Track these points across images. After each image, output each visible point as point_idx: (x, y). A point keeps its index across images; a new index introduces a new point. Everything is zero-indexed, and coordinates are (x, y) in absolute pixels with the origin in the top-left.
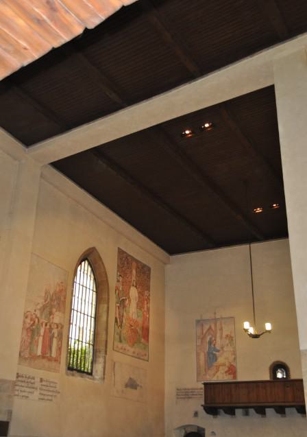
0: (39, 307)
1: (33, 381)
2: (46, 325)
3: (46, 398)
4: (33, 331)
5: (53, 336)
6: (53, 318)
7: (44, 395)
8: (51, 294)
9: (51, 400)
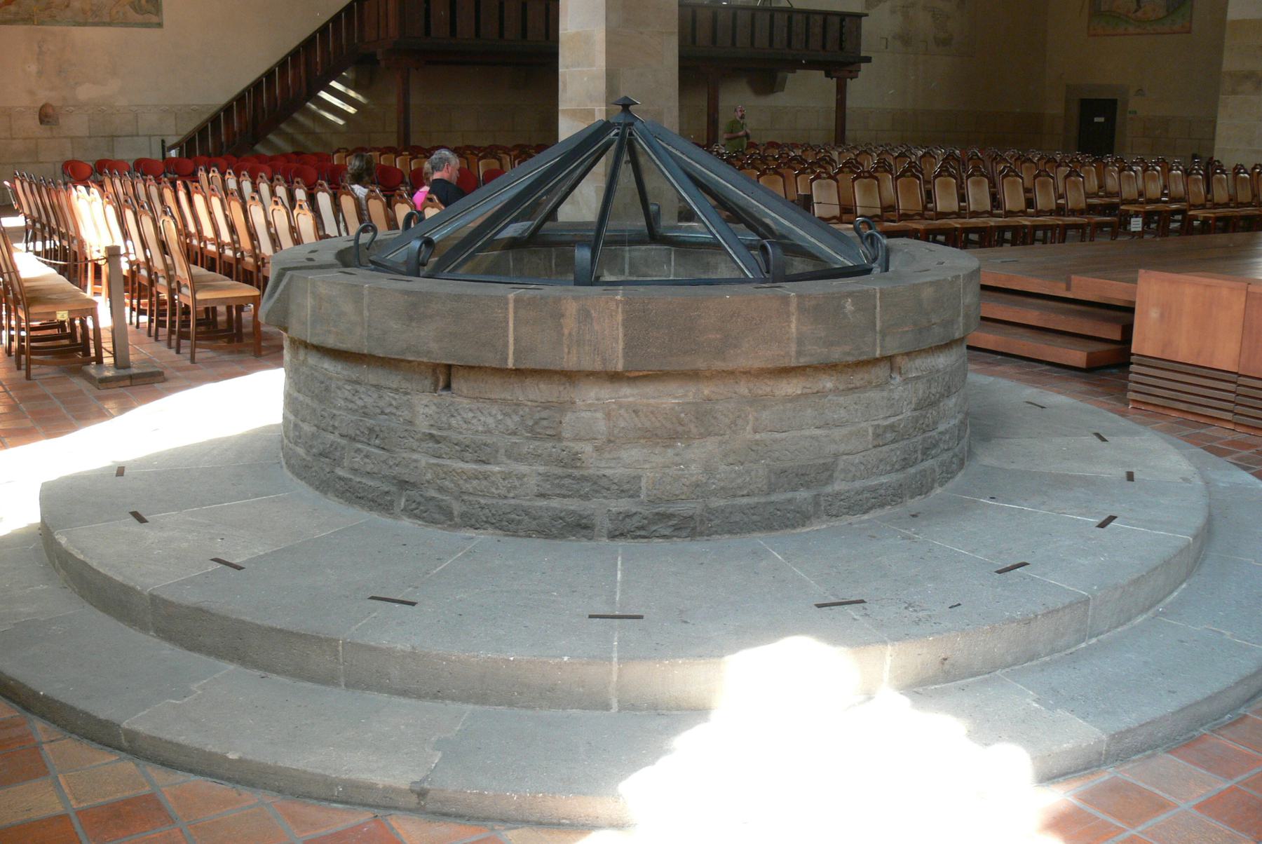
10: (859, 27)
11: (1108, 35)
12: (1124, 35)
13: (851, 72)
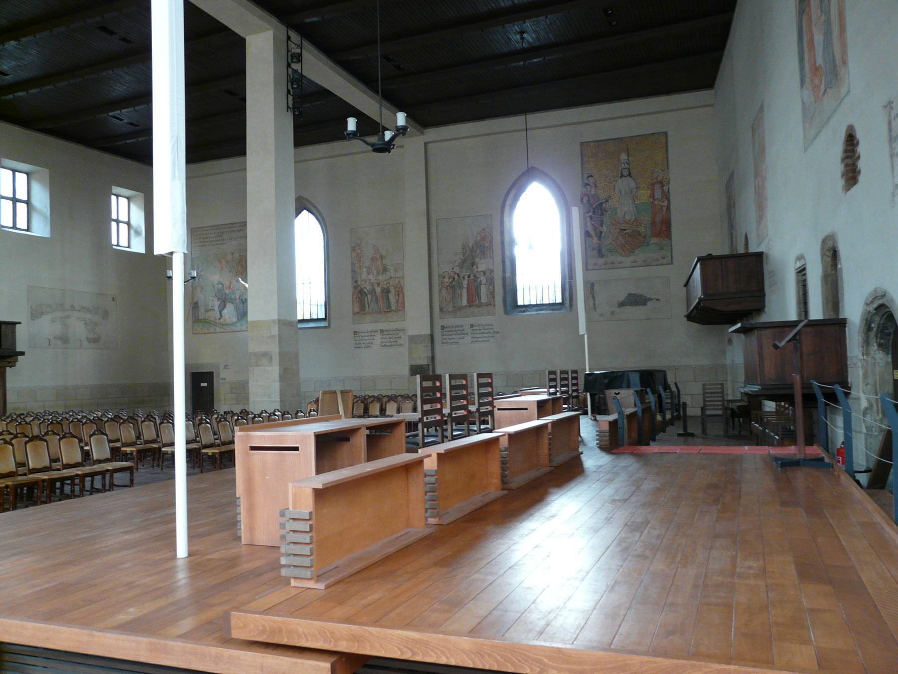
0: (457, 264)
1: (461, 329)
2: (469, 277)
3: (480, 340)
4: (453, 287)
5: (481, 284)
6: (477, 267)
7: (478, 338)
8: (471, 246)
9: (488, 341)
10: (13, 333)
11: (205, 333)
12: (215, 333)
13: (10, 362)
